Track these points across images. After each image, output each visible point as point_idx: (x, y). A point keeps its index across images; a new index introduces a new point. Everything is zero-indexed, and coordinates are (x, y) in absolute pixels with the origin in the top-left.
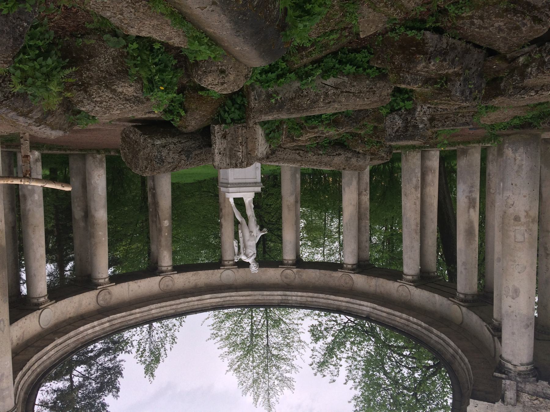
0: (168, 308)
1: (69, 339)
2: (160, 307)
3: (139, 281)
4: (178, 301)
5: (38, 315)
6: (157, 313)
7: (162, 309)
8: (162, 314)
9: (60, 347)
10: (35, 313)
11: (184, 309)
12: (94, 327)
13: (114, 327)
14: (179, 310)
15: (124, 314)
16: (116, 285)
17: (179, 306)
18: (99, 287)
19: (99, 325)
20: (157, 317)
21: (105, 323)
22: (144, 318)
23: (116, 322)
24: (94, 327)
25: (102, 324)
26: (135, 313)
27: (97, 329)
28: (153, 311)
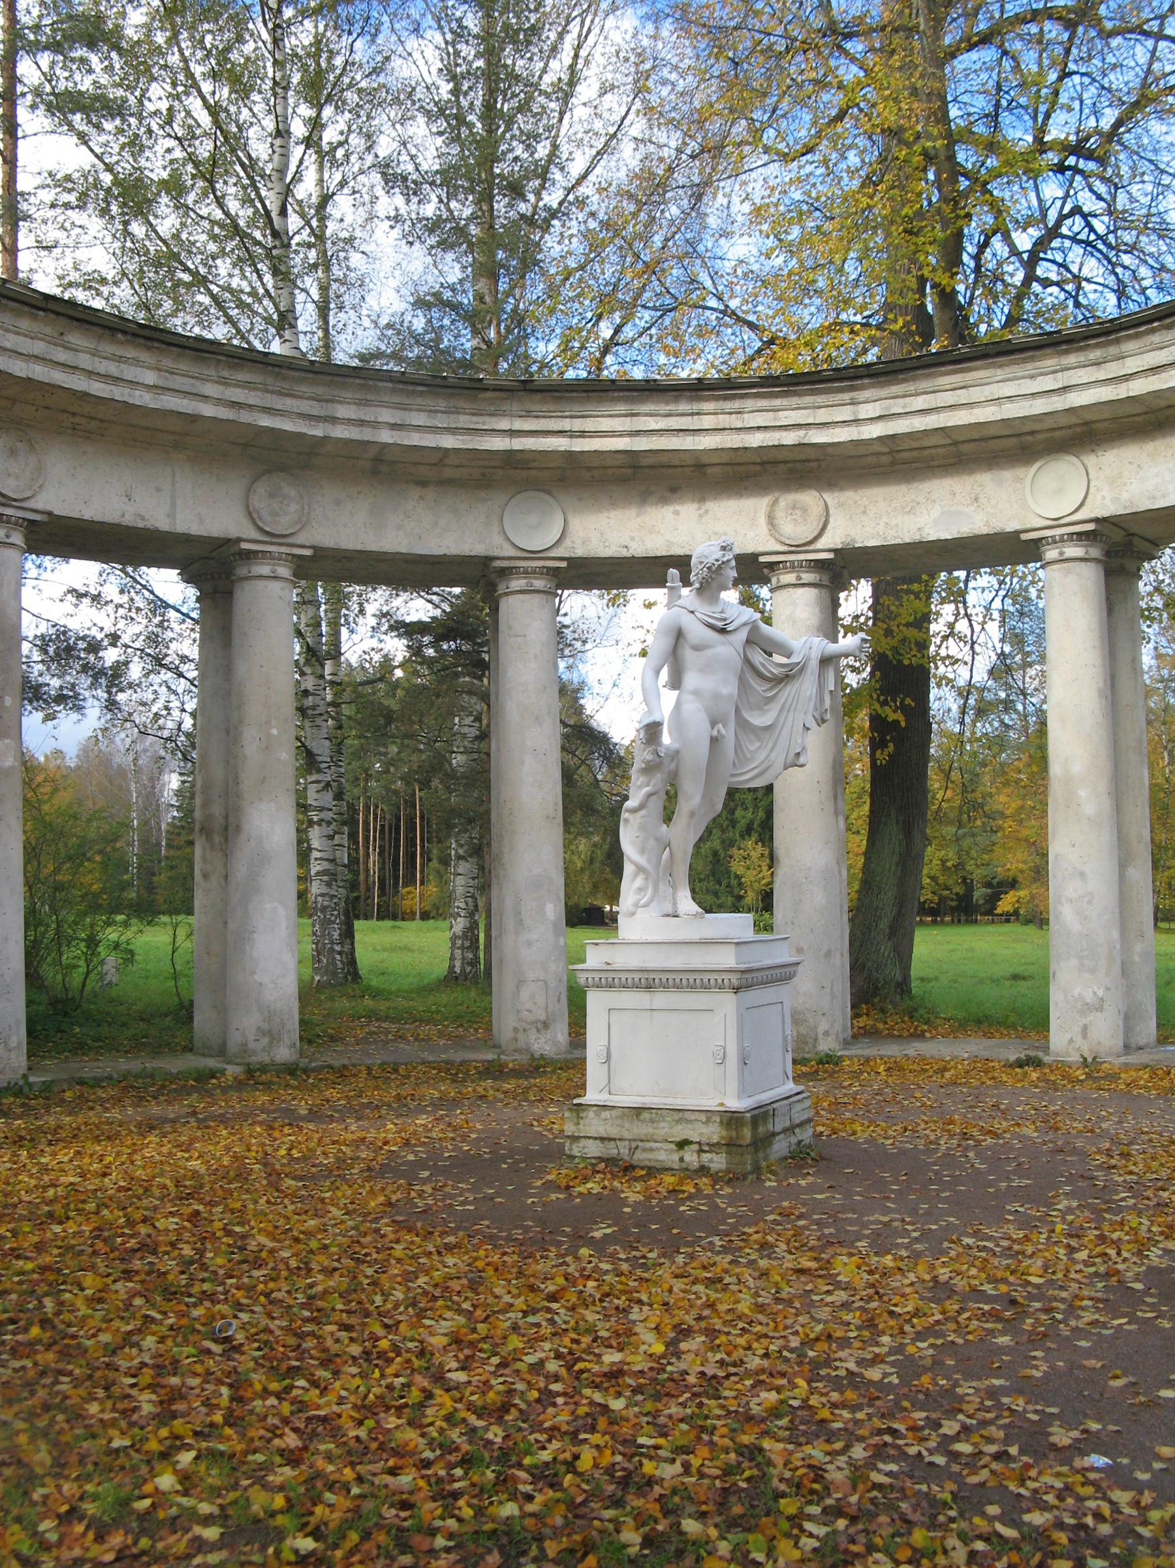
0: (84, 360)
1: (513, 433)
2: (117, 380)
3: (128, 520)
4: (39, 372)
5: (568, 542)
6: (137, 362)
7: (112, 368)
8: (120, 351)
9: (566, 424)
10: (580, 552)
11: (25, 324)
12: (394, 427)
13: (320, 390)
14: (48, 330)
15: (265, 421)
16: (239, 540)
17: (38, 347)
18: (307, 552)
19: (375, 425)
20: (149, 348)
21: (349, 422)
22: (195, 370)
23: (306, 406)
24: (394, 427)
25: (362, 423)
26: (219, 402)
27: (386, 415)
28: (150, 377)
